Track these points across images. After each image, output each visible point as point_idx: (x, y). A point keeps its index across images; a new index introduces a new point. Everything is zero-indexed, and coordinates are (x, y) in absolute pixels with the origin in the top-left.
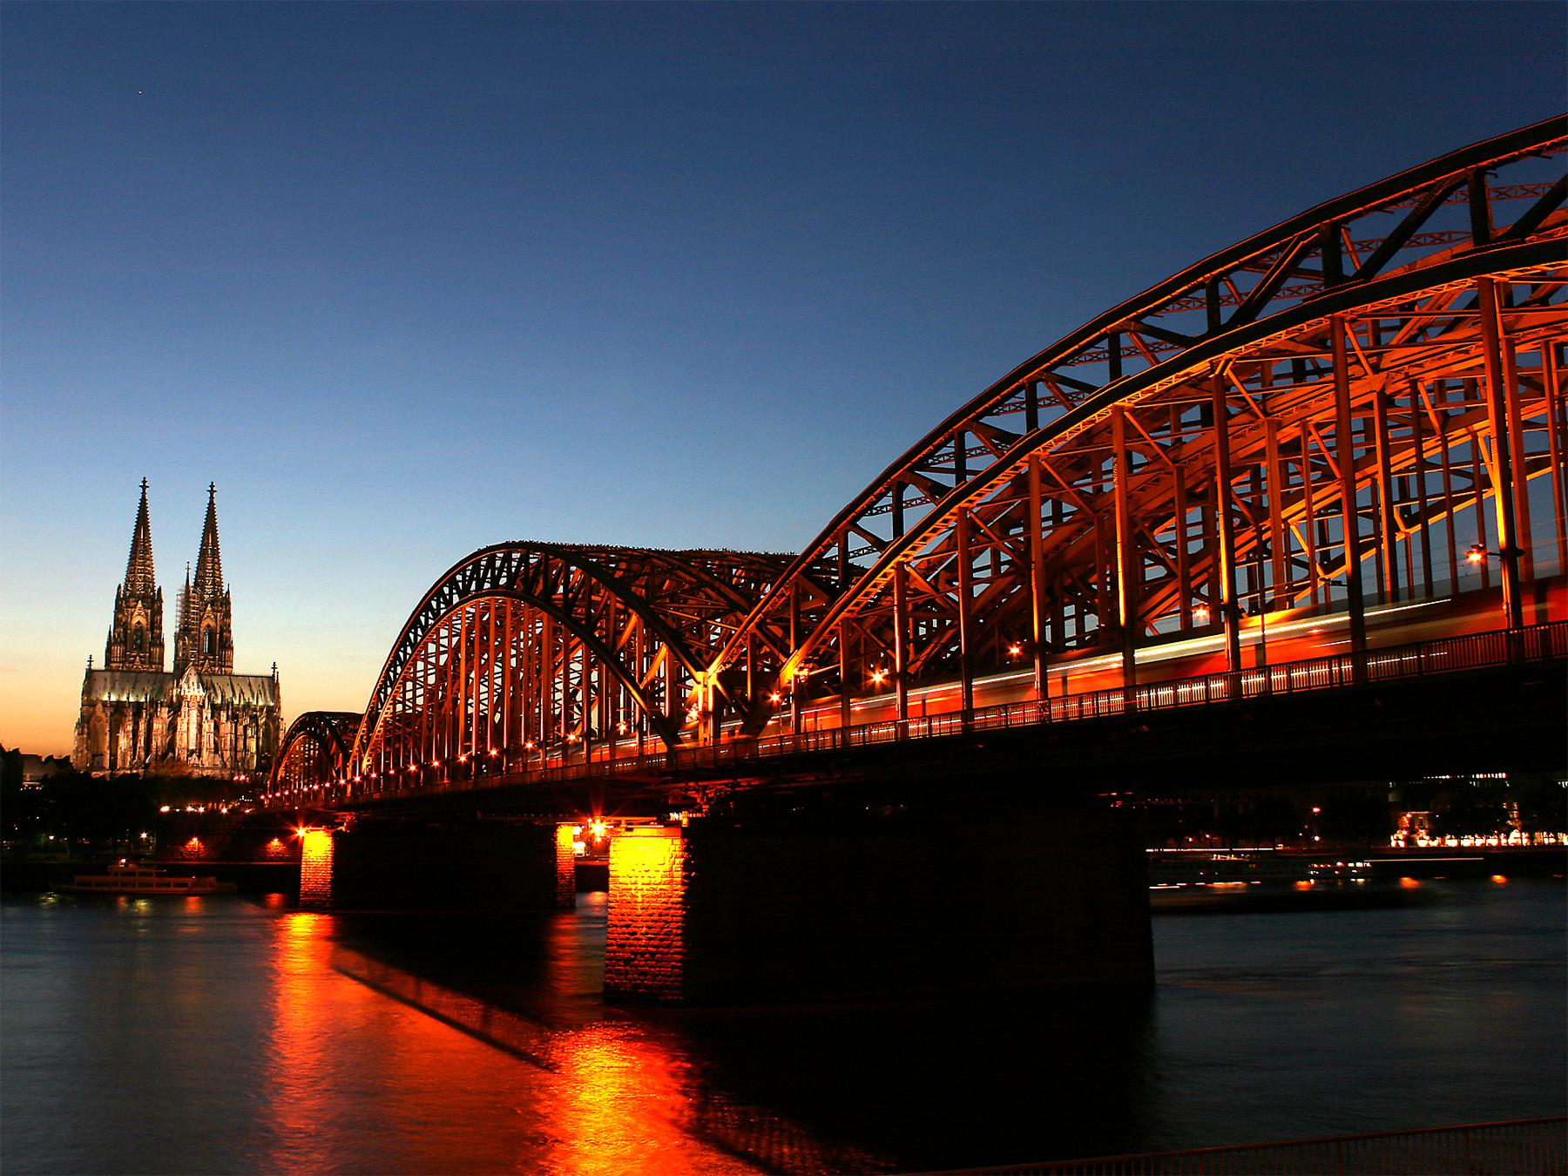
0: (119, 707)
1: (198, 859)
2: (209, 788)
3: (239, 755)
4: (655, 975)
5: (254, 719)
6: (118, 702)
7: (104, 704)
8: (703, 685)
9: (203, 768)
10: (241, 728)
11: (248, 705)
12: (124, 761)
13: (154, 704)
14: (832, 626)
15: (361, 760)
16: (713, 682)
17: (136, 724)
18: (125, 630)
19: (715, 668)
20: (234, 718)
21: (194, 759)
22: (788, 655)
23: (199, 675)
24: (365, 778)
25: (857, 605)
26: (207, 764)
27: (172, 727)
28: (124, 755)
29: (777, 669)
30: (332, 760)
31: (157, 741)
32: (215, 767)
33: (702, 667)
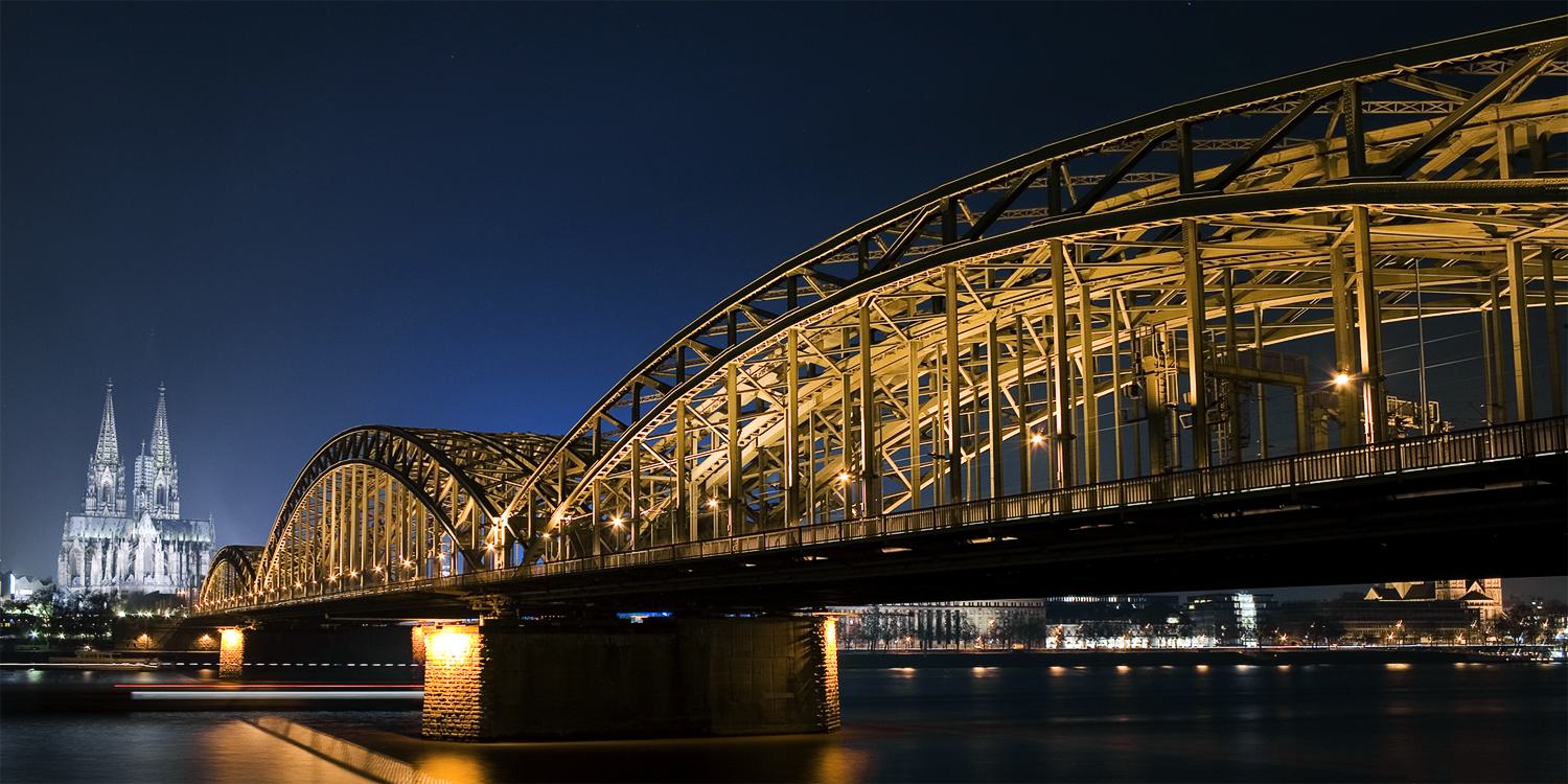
0: (91, 542)
1: (147, 649)
2: (155, 599)
4: (459, 730)
8: (499, 527)
14: (587, 486)
15: (264, 580)
16: (505, 523)
19: (506, 515)
22: (556, 506)
25: (606, 470)
26: (159, 584)
27: (132, 557)
28: (96, 576)
29: (550, 515)
30: (244, 580)
31: (122, 566)
32: (165, 585)
33: (496, 514)
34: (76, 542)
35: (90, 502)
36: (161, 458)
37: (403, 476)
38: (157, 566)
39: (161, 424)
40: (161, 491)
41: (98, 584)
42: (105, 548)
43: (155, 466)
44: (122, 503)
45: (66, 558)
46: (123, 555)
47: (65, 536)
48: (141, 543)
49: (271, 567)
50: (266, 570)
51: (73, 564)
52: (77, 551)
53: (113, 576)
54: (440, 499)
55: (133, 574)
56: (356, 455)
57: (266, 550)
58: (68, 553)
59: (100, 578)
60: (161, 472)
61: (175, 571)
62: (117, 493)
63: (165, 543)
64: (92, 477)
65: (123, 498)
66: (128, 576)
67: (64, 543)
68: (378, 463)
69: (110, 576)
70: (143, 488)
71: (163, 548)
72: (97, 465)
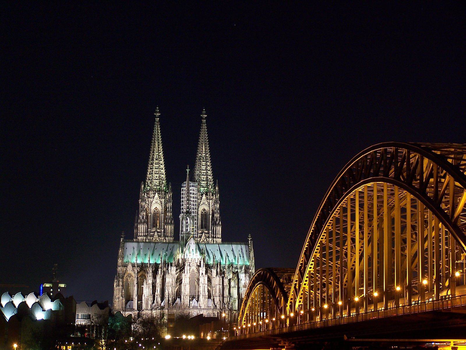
0: (143, 267)
3: (226, 300)
5: (236, 274)
6: (142, 264)
7: (133, 266)
9: (201, 309)
10: (226, 281)
11: (231, 265)
12: (147, 304)
13: (167, 265)
15: (295, 302)
17: (154, 277)
18: (147, 216)
20: (222, 274)
21: (194, 303)
23: (198, 244)
24: (297, 314)
26: (203, 307)
27: (179, 281)
30: (277, 302)
31: (170, 290)
32: (208, 308)
34: (130, 266)
35: (142, 228)
36: (203, 183)
37: (420, 193)
38: (201, 289)
39: (204, 151)
40: (205, 215)
41: (149, 308)
42: (155, 274)
43: (199, 191)
44: (170, 228)
45: (121, 283)
46: (170, 280)
47: (120, 261)
48: (187, 268)
49: (302, 289)
50: (297, 291)
51: (126, 288)
52: (130, 276)
53: (162, 300)
54: (456, 215)
55: (180, 298)
56: (376, 174)
57: (297, 271)
58: (123, 278)
59: (150, 303)
60: (204, 197)
61: (217, 294)
62: (165, 218)
63: (208, 267)
64: (143, 204)
65: (171, 224)
66: (175, 300)
67: (119, 269)
68: (396, 181)
69: (159, 299)
70: (188, 213)
71: (206, 272)
72: (147, 192)
